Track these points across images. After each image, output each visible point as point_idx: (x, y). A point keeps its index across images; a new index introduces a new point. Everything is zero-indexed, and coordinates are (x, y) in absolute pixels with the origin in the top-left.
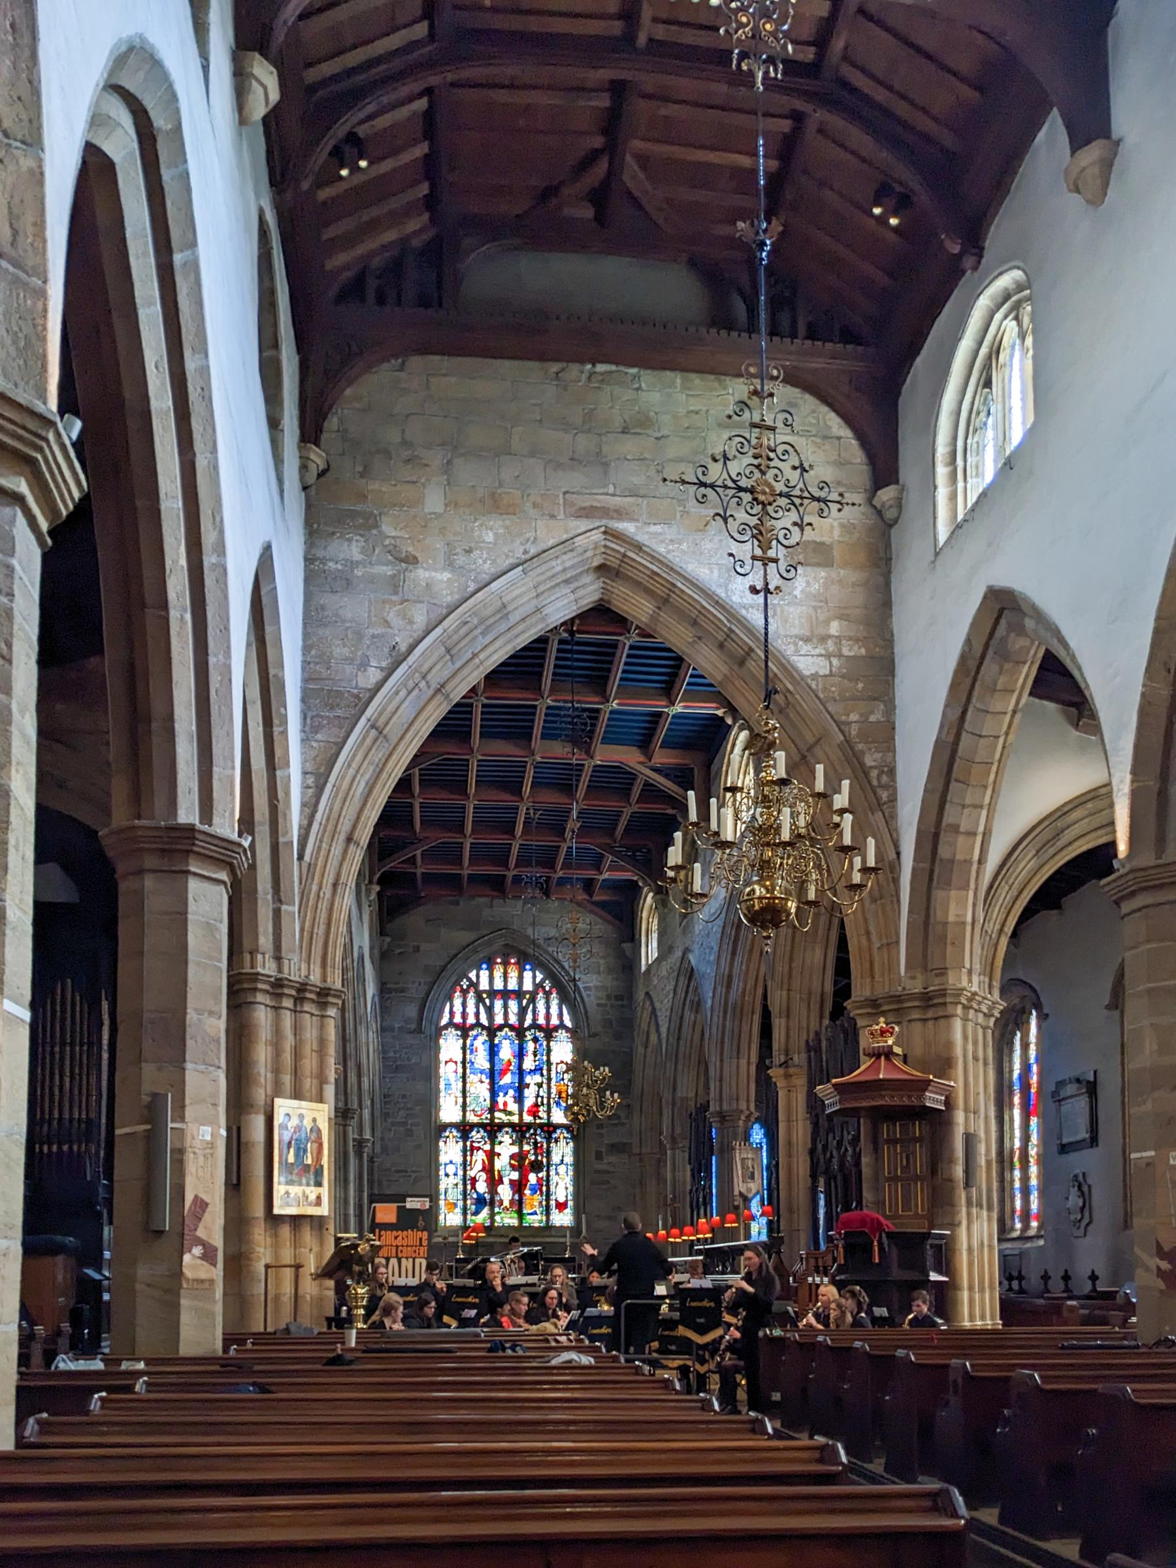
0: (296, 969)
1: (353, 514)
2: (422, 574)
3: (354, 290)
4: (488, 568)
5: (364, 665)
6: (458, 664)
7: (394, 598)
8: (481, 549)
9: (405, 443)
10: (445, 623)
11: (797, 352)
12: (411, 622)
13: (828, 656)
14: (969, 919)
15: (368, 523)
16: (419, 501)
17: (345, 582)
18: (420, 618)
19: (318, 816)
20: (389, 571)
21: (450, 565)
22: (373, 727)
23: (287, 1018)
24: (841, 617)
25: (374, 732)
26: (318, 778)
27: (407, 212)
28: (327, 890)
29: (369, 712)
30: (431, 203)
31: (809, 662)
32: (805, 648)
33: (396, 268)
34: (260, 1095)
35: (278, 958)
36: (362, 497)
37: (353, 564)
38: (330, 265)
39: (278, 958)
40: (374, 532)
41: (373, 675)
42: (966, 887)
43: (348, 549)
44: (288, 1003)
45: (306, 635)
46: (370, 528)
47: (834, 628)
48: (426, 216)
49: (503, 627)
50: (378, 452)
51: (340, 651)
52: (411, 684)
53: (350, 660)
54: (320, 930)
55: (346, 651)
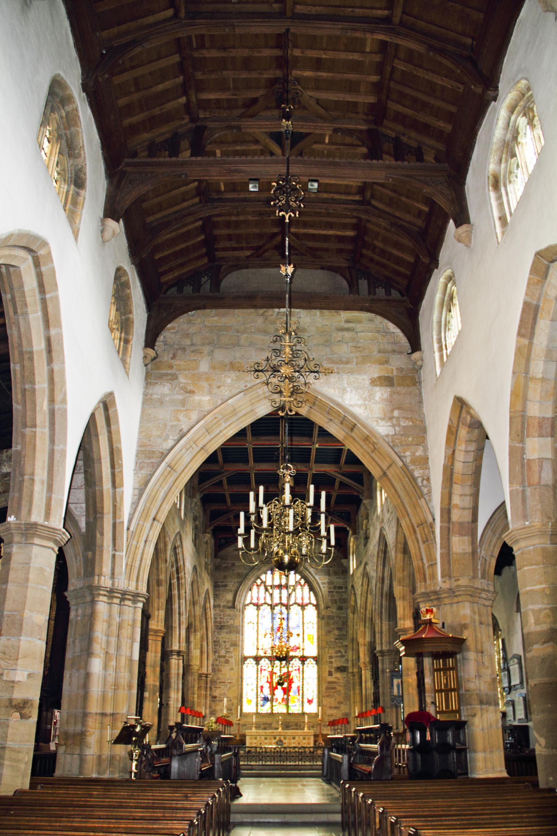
0: (122, 583)
2: (197, 398)
4: (227, 394)
6: (212, 436)
7: (182, 409)
8: (225, 386)
10: (206, 419)
12: (190, 419)
13: (393, 426)
15: (174, 377)
16: (197, 368)
17: (161, 402)
18: (194, 416)
19: (139, 509)
20: (181, 397)
21: (210, 393)
22: (169, 466)
23: (116, 608)
24: (399, 408)
25: (169, 469)
28: (142, 544)
29: (167, 459)
31: (383, 429)
32: (382, 423)
40: (176, 381)
41: (170, 443)
43: (163, 389)
44: (117, 601)
45: (141, 427)
46: (173, 380)
47: (396, 413)
49: (234, 419)
50: (180, 349)
51: (155, 433)
52: (188, 446)
53: (160, 437)
55: (159, 433)
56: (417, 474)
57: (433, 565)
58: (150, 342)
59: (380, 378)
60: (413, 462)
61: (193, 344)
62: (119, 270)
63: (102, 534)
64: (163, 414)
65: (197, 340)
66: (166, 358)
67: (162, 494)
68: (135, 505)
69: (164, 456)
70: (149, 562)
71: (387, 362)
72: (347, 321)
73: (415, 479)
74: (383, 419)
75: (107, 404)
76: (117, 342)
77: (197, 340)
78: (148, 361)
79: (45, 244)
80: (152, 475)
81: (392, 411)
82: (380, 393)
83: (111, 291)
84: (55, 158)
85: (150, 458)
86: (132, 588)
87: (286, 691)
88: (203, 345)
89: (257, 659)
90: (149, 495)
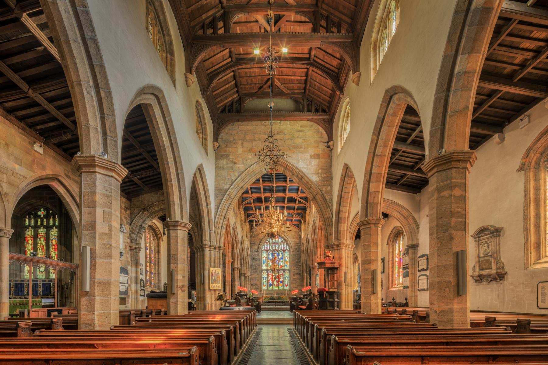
0: (214, 243)
1: (224, 155)
2: (237, 166)
3: (223, 111)
4: (250, 163)
5: (226, 184)
9: (234, 140)
11: (311, 115)
13: (319, 177)
14: (346, 229)
15: (227, 156)
17: (223, 168)
18: (237, 174)
20: (231, 165)
21: (243, 163)
23: (212, 253)
24: (321, 169)
26: (218, 207)
27: (233, 94)
29: (227, 193)
30: (237, 92)
31: (315, 179)
32: (314, 176)
33: (231, 105)
34: (207, 267)
35: (210, 241)
36: (226, 151)
37: (224, 165)
38: (218, 106)
39: (210, 241)
41: (228, 186)
42: (345, 223)
43: (223, 162)
44: (212, 250)
47: (320, 171)
48: (237, 95)
54: (219, 235)
56: (327, 198)
57: (331, 235)
58: (216, 139)
59: (314, 154)
60: (326, 193)
61: (234, 140)
62: (197, 102)
63: (204, 224)
64: (224, 173)
65: (236, 138)
66: (223, 146)
67: (226, 208)
68: (216, 212)
69: (226, 191)
70: (224, 235)
71: (317, 147)
72: (301, 127)
73: (326, 200)
74: (314, 174)
75: (200, 169)
76: (201, 139)
77: (236, 138)
78: (216, 148)
79: (161, 91)
80: (222, 200)
81: (319, 170)
82: (314, 162)
83: (195, 114)
84: (157, 38)
85: (221, 192)
86: (218, 244)
87: (278, 282)
88: (239, 140)
89: (267, 270)
90: (221, 208)
